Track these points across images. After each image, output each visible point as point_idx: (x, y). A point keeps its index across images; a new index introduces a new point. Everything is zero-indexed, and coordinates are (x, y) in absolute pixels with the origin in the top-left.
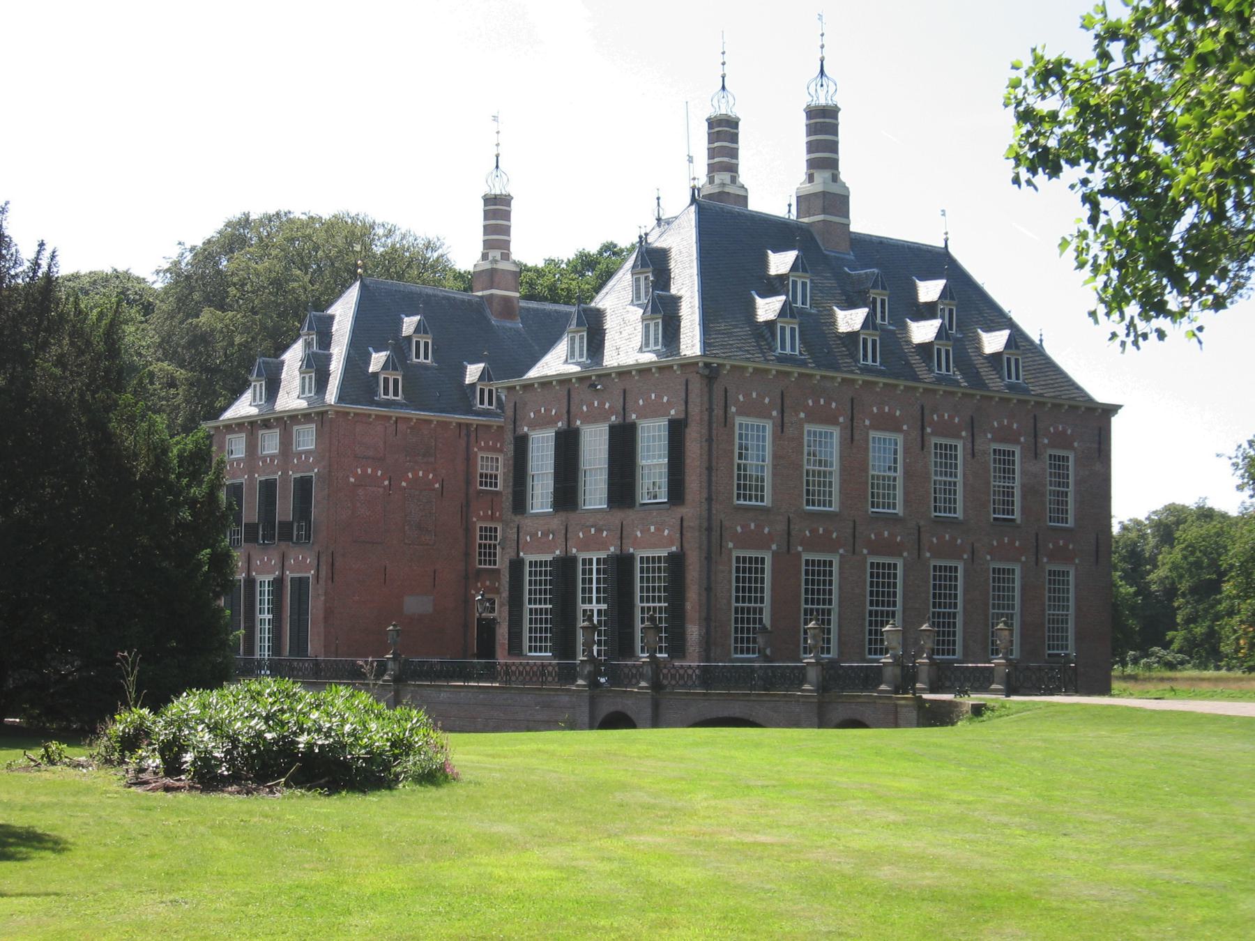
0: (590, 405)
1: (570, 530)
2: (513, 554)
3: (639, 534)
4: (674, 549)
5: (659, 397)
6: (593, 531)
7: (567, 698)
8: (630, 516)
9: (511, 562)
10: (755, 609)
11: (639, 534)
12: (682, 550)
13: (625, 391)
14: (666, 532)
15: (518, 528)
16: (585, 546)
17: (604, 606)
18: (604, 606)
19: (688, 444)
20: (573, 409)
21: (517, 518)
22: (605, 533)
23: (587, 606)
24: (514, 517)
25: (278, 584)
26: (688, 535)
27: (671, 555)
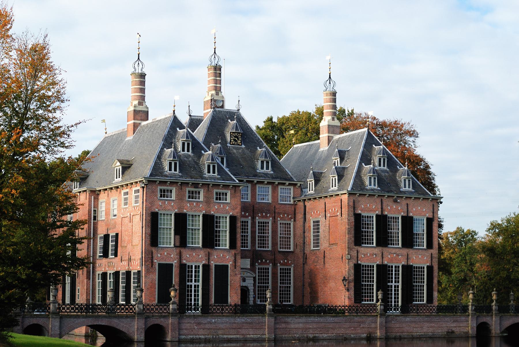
1: (384, 254)
2: (355, 262)
3: (414, 258)
4: (428, 264)
5: (422, 209)
6: (395, 255)
7: (464, 318)
8: (410, 251)
9: (355, 265)
10: (370, 285)
11: (414, 258)
12: (432, 264)
13: (407, 204)
14: (425, 258)
15: (357, 251)
17: (390, 284)
18: (390, 284)
19: (434, 227)
20: (384, 207)
21: (356, 247)
22: (400, 257)
23: (397, 284)
24: (354, 247)
25: (206, 268)
26: (434, 260)
27: (428, 267)
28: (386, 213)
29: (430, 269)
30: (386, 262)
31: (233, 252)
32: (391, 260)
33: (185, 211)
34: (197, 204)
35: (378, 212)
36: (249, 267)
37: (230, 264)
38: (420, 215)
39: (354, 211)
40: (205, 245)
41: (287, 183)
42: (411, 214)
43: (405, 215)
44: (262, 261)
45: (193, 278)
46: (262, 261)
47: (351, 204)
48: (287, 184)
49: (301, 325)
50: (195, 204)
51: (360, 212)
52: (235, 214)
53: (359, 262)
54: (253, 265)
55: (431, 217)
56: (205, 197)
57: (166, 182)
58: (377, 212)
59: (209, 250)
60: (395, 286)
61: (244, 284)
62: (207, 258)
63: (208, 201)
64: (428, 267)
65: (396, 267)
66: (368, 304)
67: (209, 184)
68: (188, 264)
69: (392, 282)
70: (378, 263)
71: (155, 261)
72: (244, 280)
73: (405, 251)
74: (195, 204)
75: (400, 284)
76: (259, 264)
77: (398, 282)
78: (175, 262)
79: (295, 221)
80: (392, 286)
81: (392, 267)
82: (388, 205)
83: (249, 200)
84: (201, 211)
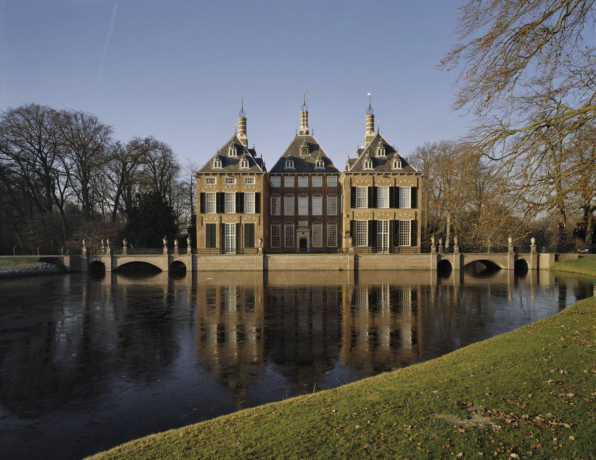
0: (381, 181)
6: (383, 214)
15: (353, 212)
16: (380, 217)
23: (386, 233)
27: (412, 221)
28: (376, 185)
29: (414, 223)
30: (376, 219)
31: (258, 215)
32: (380, 217)
33: (223, 191)
34: (232, 186)
35: (371, 185)
36: (307, 225)
37: (255, 223)
38: (406, 185)
39: (351, 186)
40: (237, 211)
41: (332, 174)
42: (397, 185)
43: (393, 186)
44: (316, 222)
45: (230, 232)
46: (316, 222)
47: (349, 180)
48: (332, 174)
49: (285, 261)
50: (230, 186)
51: (355, 185)
52: (259, 192)
53: (354, 219)
54: (310, 224)
55: (416, 186)
56: (237, 181)
57: (209, 174)
58: (369, 185)
59: (240, 214)
60: (384, 235)
61: (303, 236)
62: (239, 219)
63: (239, 184)
64: (412, 221)
65: (384, 221)
66: (363, 247)
67: (240, 174)
68: (226, 223)
69: (381, 232)
70: (369, 219)
71: (204, 222)
72: (303, 233)
73: (393, 210)
74: (230, 186)
75: (388, 233)
76: (314, 224)
77: (387, 232)
78: (217, 223)
79: (338, 197)
80: (381, 235)
81: (382, 222)
82: (378, 180)
83: (307, 186)
84: (234, 190)
